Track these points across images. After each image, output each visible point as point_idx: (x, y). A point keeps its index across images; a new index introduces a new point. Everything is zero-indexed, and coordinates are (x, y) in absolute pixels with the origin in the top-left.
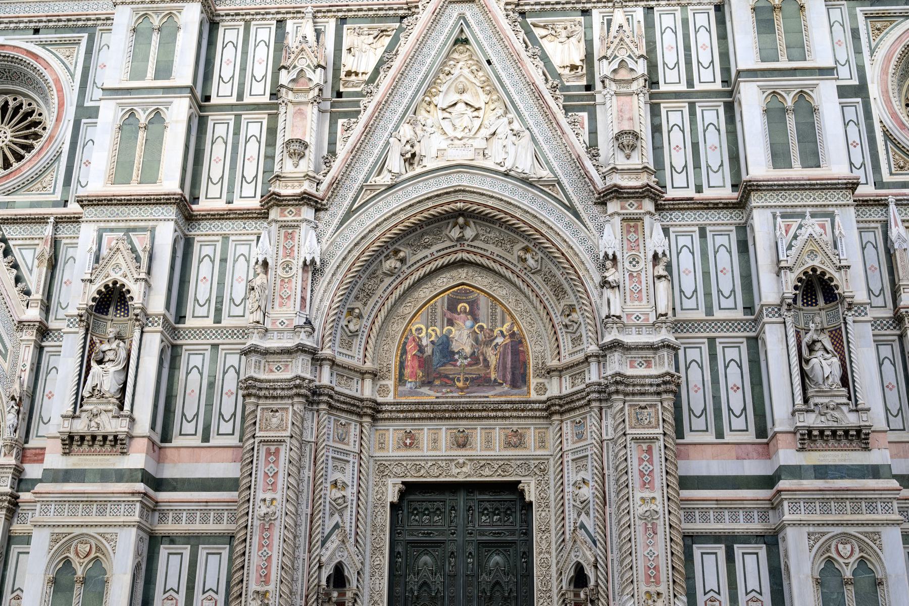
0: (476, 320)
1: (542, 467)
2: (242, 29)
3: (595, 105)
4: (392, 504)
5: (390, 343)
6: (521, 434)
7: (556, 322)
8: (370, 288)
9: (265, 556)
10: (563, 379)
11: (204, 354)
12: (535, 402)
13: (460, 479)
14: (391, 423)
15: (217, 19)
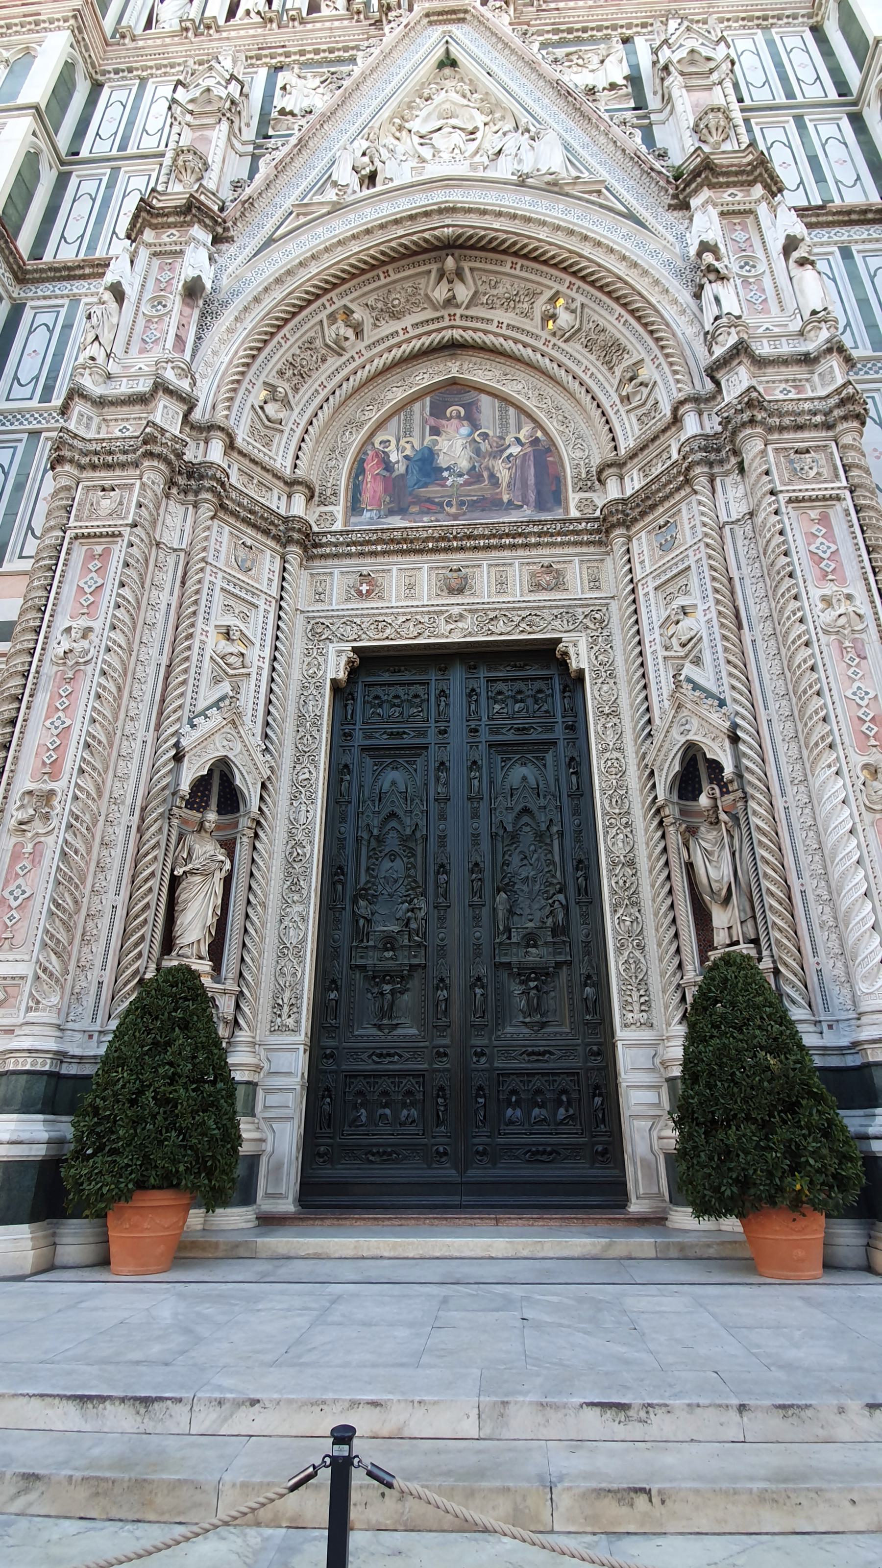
0: (475, 426)
1: (597, 616)
2: (135, 89)
3: (651, 124)
4: (334, 681)
5: (339, 457)
6: (557, 571)
7: (606, 404)
8: (304, 363)
9: (56, 728)
10: (627, 479)
11: (15, 448)
12: (578, 520)
13: (455, 638)
14: (336, 562)
15: (99, 77)
